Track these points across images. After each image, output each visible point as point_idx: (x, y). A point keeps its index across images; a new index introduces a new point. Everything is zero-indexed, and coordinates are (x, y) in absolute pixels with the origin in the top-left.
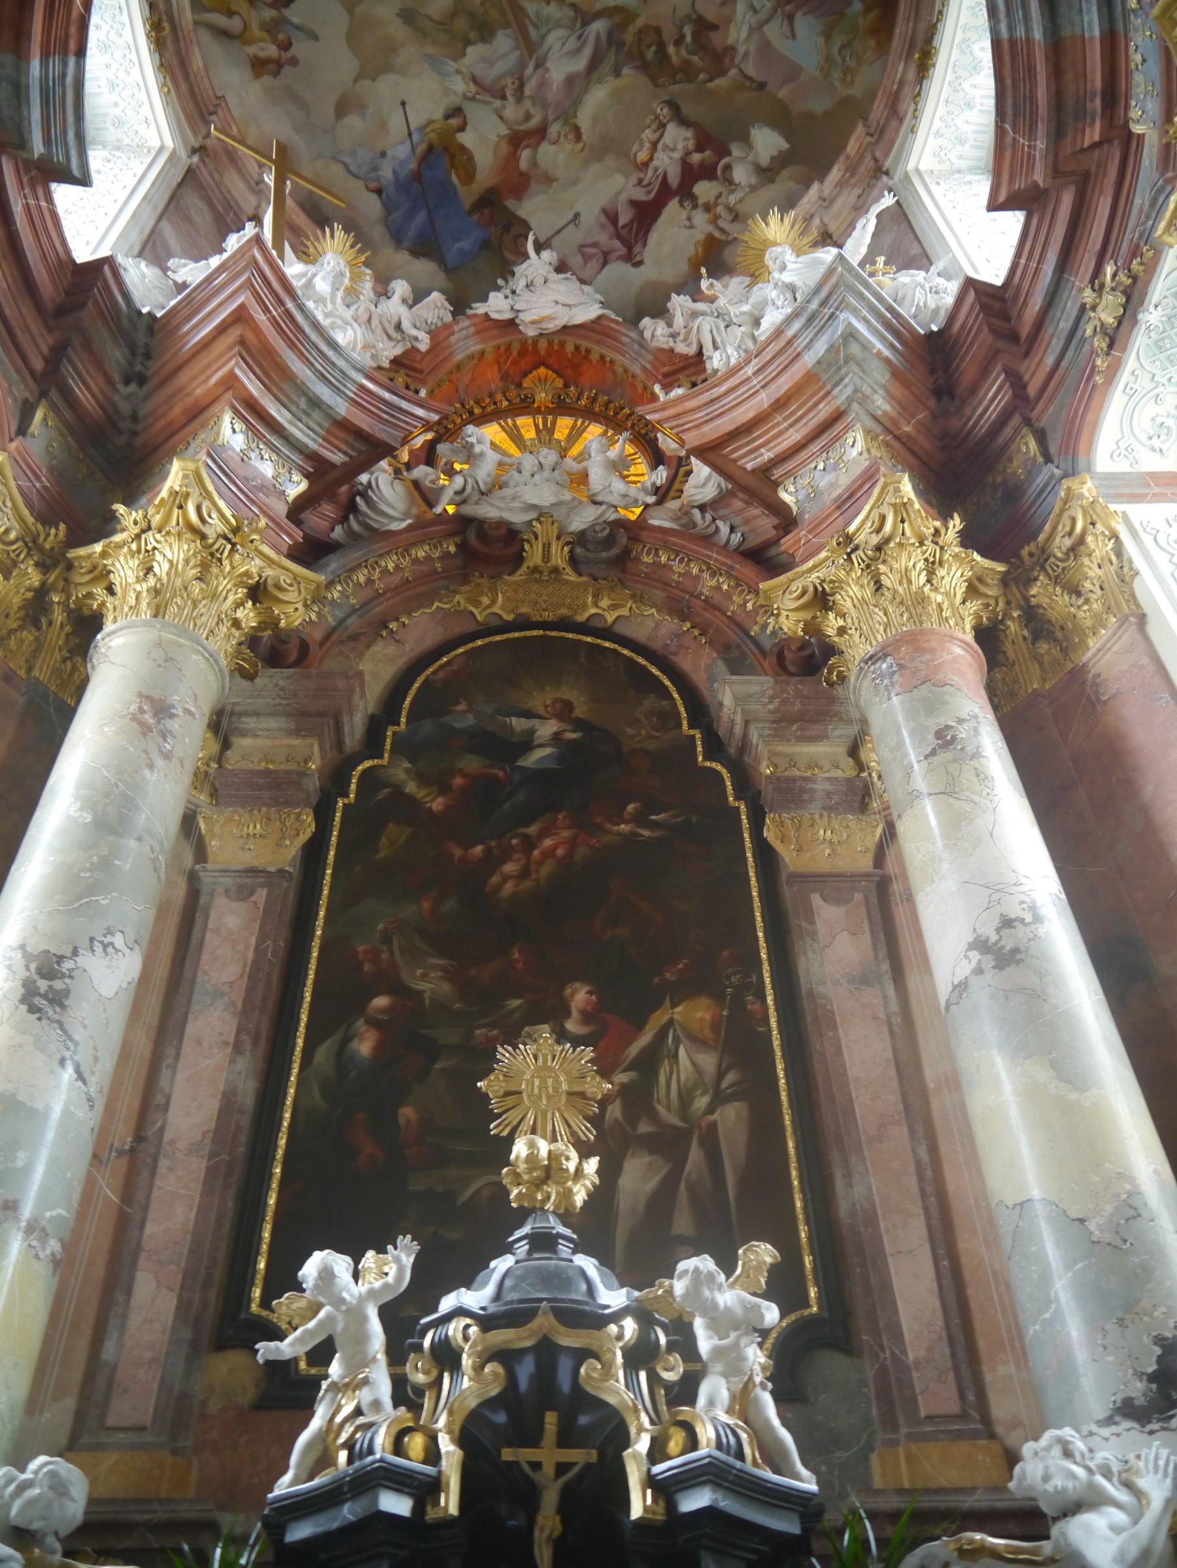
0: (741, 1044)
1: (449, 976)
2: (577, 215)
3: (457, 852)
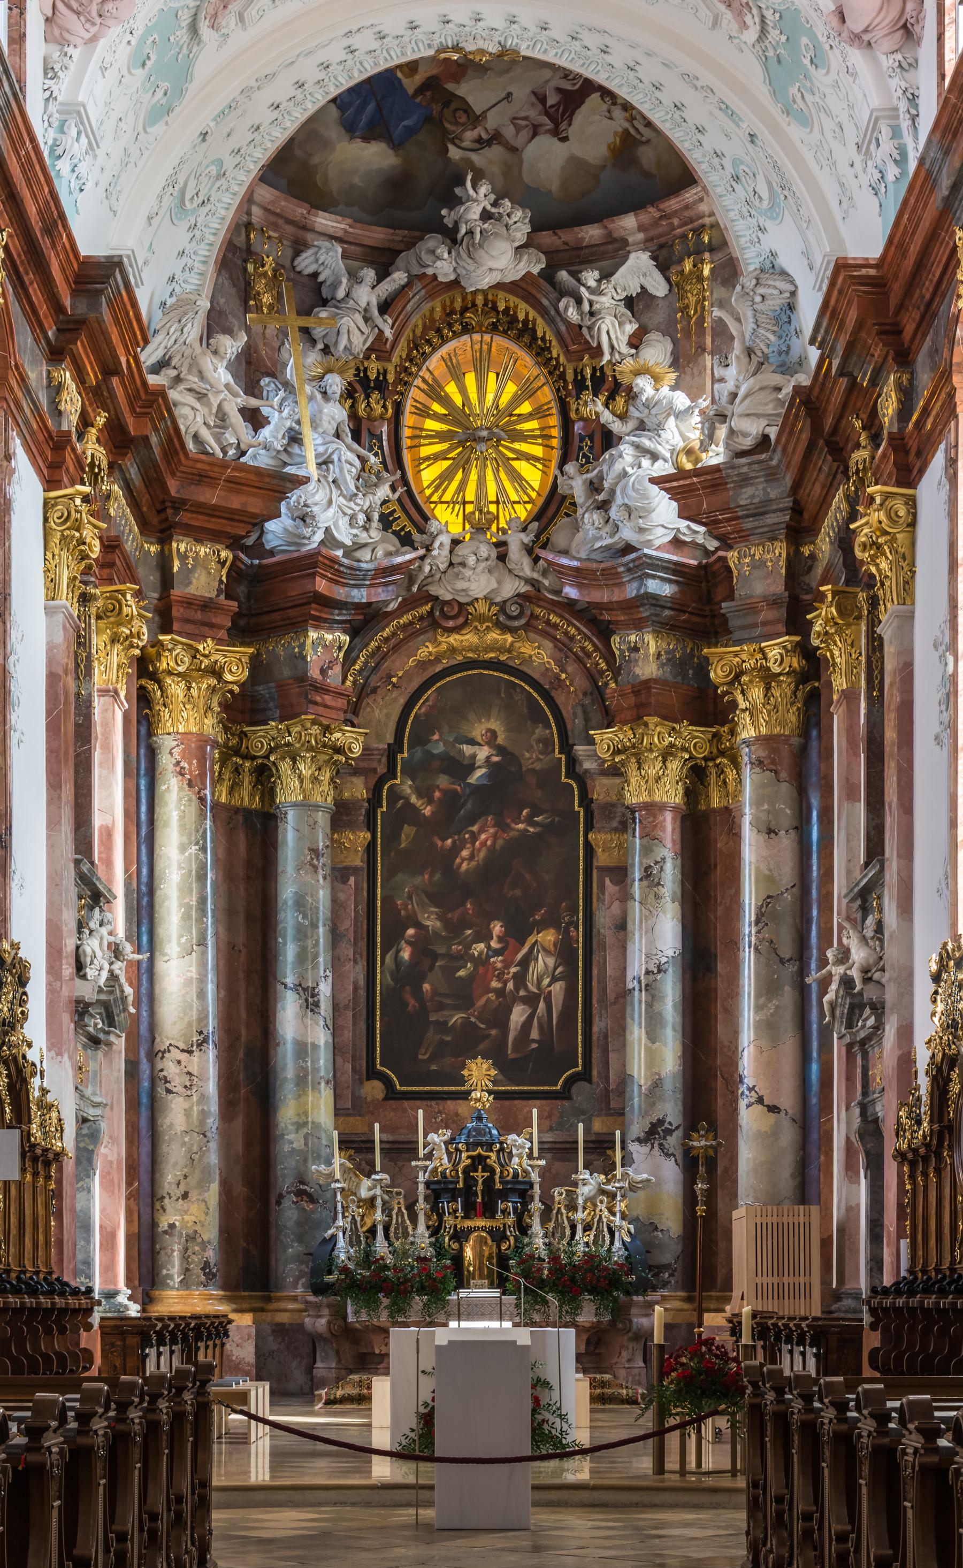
1: (440, 918)
2: (509, 95)
3: (439, 843)
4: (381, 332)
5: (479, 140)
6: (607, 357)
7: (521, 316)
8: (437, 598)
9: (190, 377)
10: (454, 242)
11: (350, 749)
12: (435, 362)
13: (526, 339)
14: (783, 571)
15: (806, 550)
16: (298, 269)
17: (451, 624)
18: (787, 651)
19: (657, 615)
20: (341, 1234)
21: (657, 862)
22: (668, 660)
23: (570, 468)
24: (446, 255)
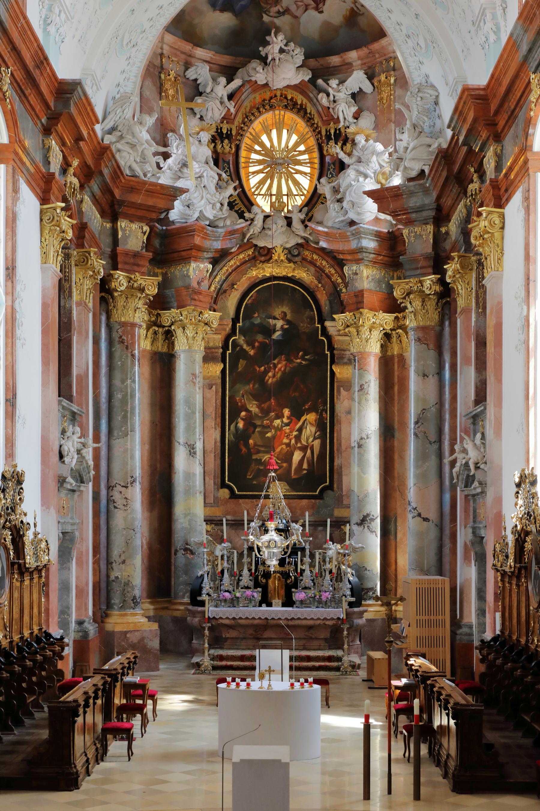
0: (321, 425)
1: (258, 407)
3: (258, 369)
4: (229, 110)
5: (279, 12)
6: (342, 124)
7: (299, 102)
8: (256, 246)
9: (128, 136)
10: (266, 64)
11: (212, 323)
12: (257, 125)
13: (302, 113)
14: (432, 241)
15: (443, 230)
16: (187, 77)
17: (263, 259)
18: (434, 283)
19: (367, 257)
20: (206, 575)
21: (366, 383)
22: (373, 279)
23: (323, 180)
24: (261, 71)
